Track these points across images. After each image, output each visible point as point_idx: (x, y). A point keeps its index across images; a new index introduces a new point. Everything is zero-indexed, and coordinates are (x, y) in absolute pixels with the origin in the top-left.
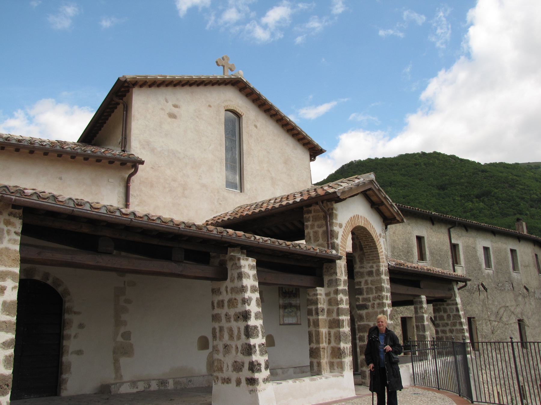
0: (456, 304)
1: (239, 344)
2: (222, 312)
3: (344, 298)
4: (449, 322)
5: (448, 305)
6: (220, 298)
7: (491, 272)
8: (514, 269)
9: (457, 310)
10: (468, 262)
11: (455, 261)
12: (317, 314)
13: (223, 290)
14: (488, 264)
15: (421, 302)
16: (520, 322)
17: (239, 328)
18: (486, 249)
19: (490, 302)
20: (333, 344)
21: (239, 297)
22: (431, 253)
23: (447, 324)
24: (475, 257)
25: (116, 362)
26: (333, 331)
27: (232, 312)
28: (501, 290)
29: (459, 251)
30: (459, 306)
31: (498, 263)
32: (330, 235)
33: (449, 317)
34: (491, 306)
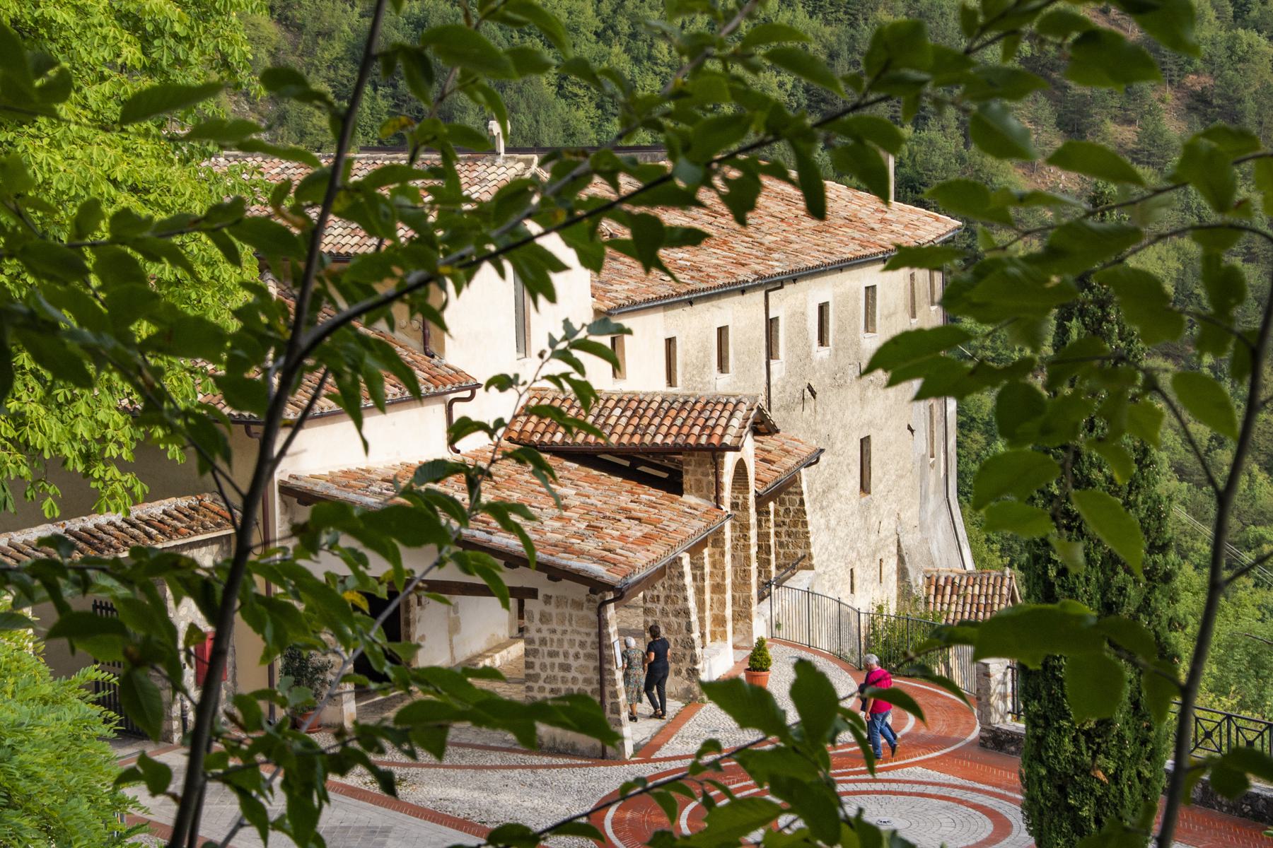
0: (802, 493)
1: (679, 637)
2: (658, 607)
3: (728, 558)
4: (787, 520)
5: (789, 493)
6: (656, 593)
7: (824, 353)
8: (867, 330)
9: (802, 502)
10: (791, 347)
11: (771, 353)
12: (703, 580)
13: (658, 585)
14: (822, 340)
15: (768, 513)
16: (865, 443)
17: (679, 625)
18: (823, 309)
19: (819, 418)
20: (716, 611)
21: (680, 595)
22: (736, 353)
23: (784, 523)
24: (803, 331)
25: (451, 641)
26: (716, 597)
27: (669, 608)
28: (840, 386)
29: (777, 331)
30: (805, 497)
31: (842, 330)
32: (719, 486)
33: (787, 511)
34: (818, 427)
